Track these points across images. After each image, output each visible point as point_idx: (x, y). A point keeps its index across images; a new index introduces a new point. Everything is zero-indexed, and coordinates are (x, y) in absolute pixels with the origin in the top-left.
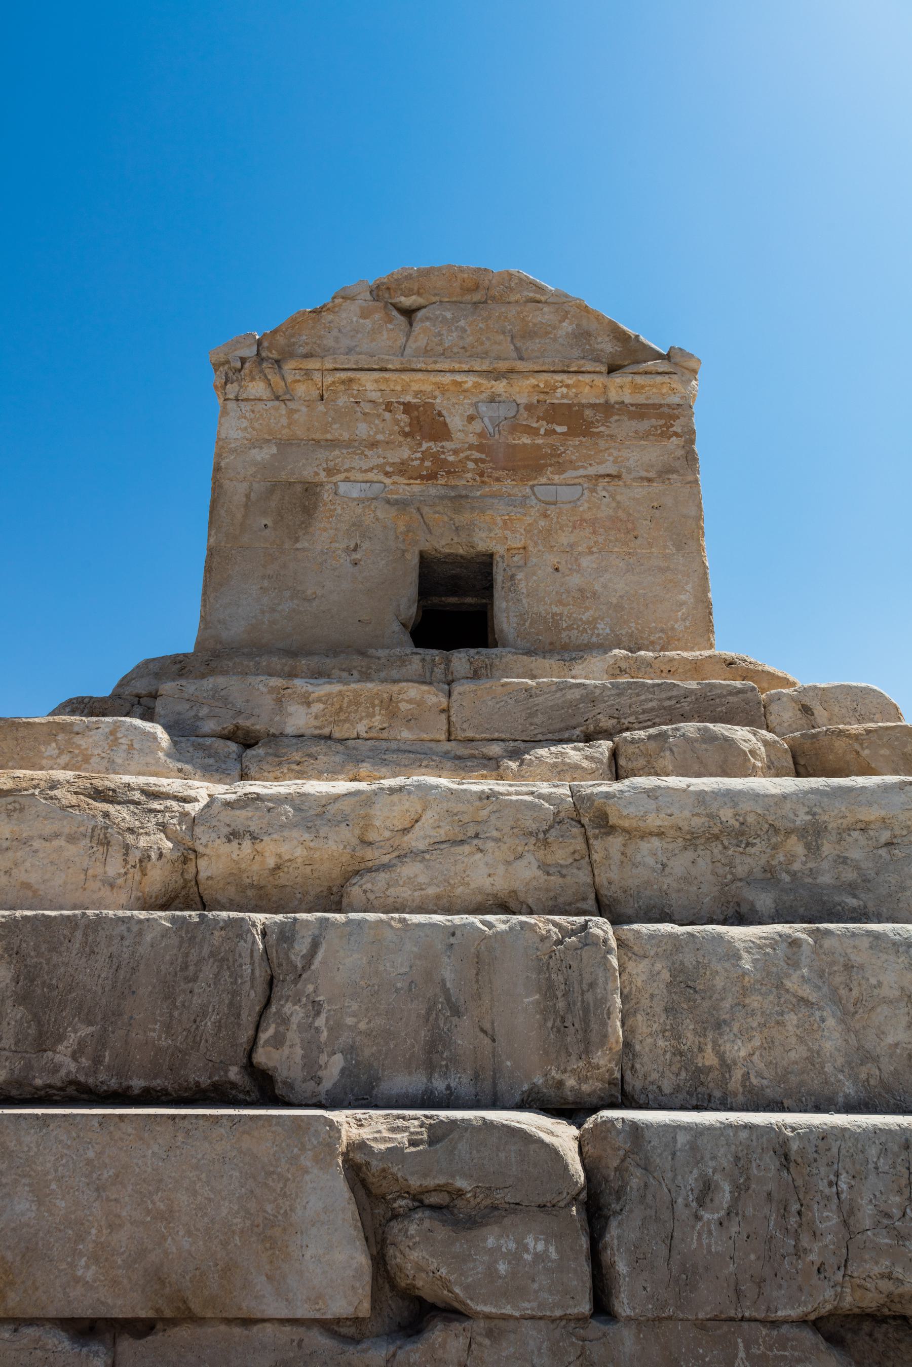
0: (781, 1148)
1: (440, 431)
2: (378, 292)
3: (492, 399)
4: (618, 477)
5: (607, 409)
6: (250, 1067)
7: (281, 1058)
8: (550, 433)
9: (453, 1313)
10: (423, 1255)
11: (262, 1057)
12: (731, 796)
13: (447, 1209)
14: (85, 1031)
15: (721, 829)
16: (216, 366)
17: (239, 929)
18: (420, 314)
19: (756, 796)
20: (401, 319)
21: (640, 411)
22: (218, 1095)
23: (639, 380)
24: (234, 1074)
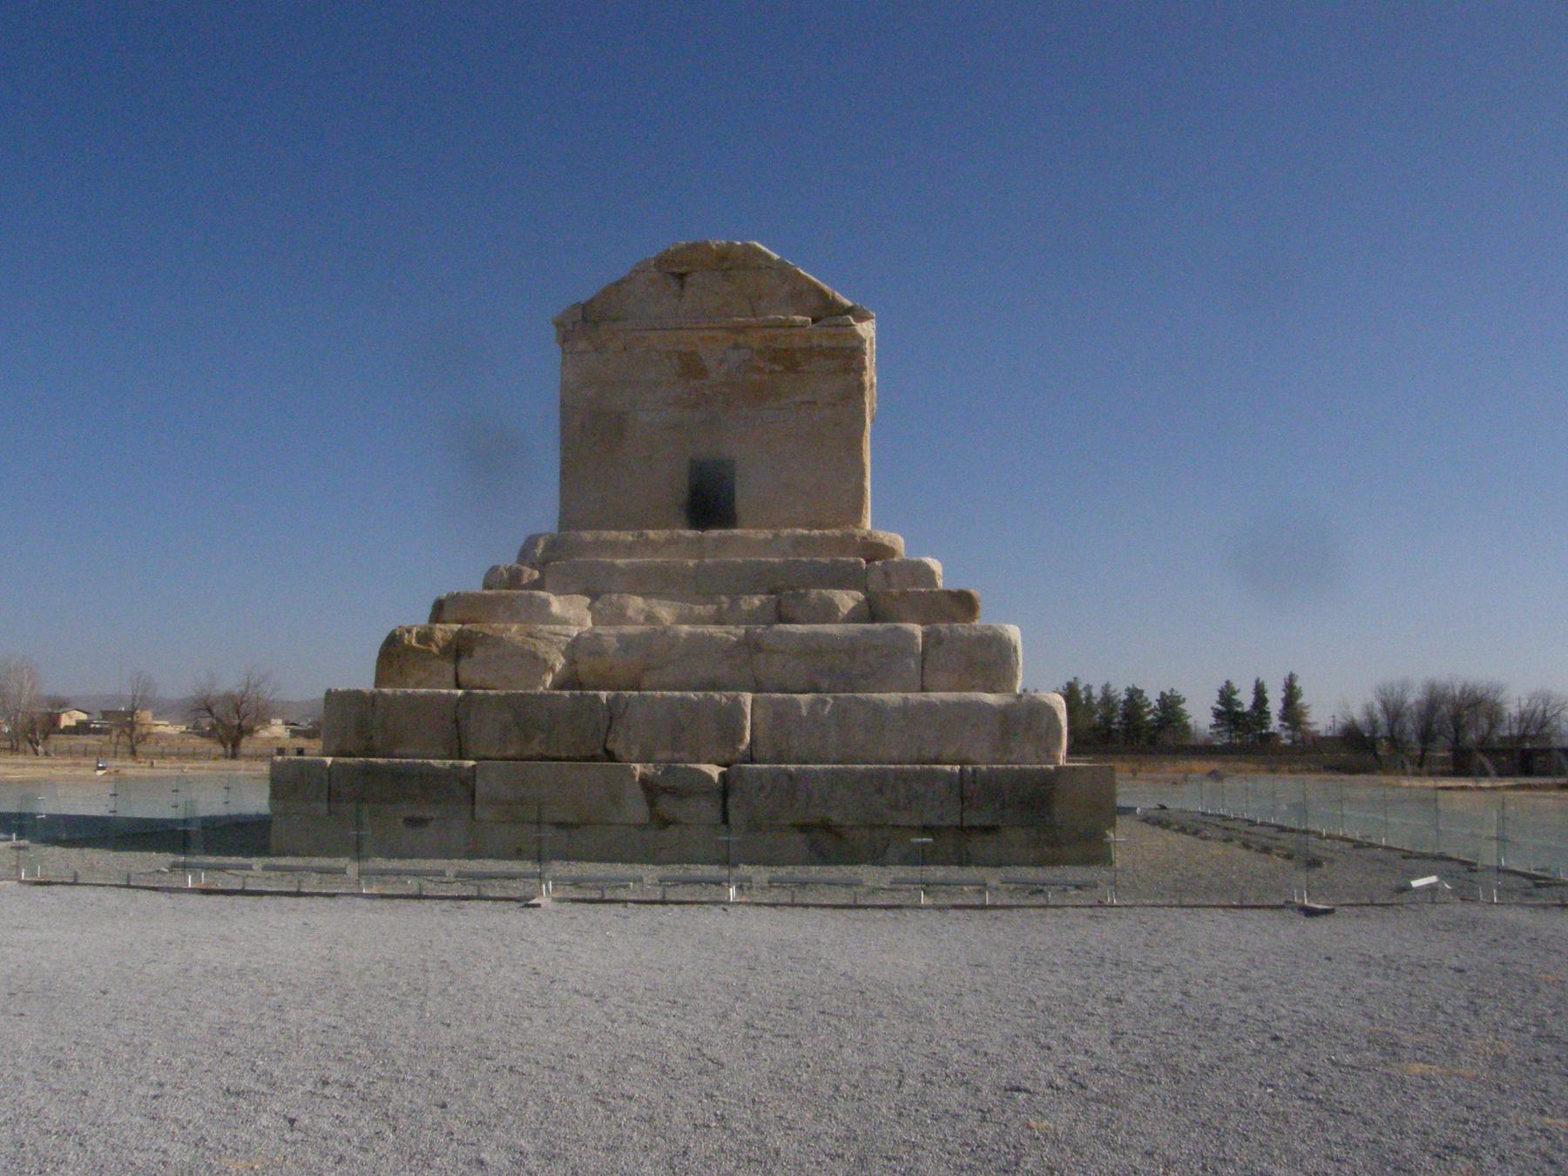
0: (790, 776)
1: (704, 373)
2: (661, 261)
3: (736, 347)
4: (815, 403)
5: (809, 352)
6: (605, 750)
7: (617, 747)
8: (772, 372)
9: (675, 822)
10: (666, 806)
11: (609, 746)
12: (816, 635)
13: (673, 792)
14: (542, 736)
15: (812, 649)
16: (557, 325)
17: (596, 696)
18: (688, 280)
19: (830, 636)
20: (675, 287)
21: (830, 354)
22: (594, 758)
23: (831, 331)
24: (600, 751)
